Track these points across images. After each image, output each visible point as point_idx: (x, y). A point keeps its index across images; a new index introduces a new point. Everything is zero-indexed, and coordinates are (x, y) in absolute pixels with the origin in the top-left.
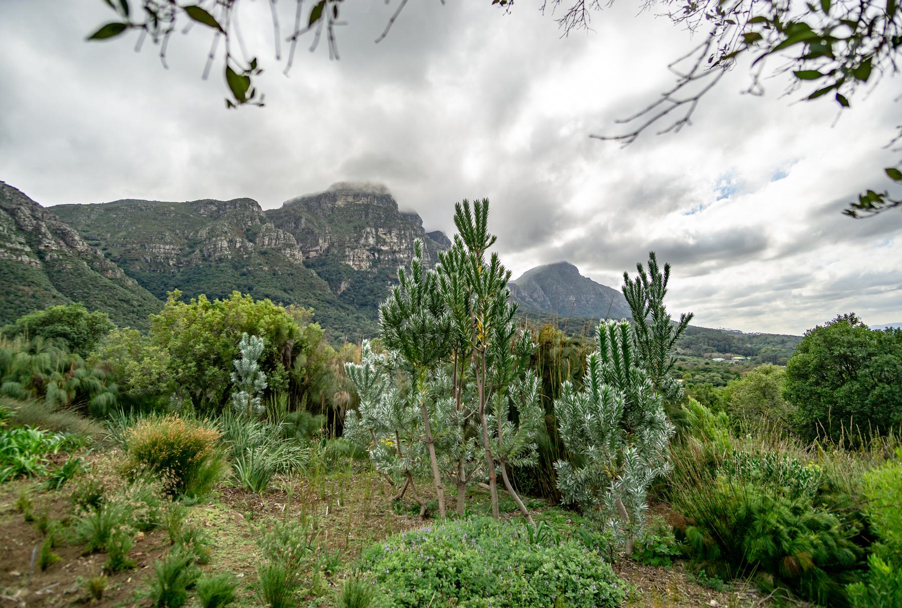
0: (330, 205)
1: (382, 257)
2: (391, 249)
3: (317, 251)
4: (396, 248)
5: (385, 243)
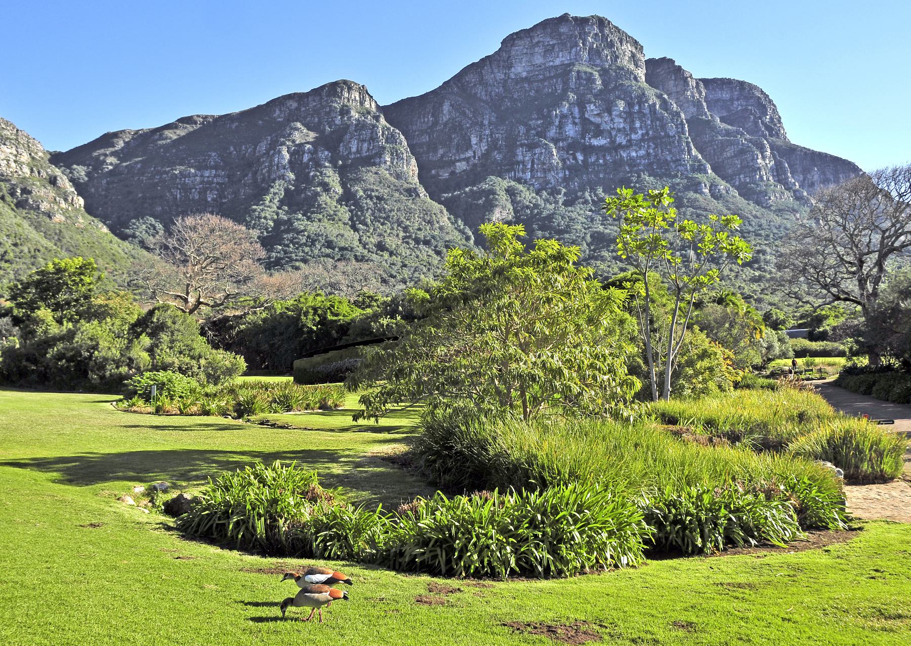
0: (500, 76)
1: (593, 159)
2: (613, 142)
3: (467, 160)
4: (621, 139)
5: (598, 132)
